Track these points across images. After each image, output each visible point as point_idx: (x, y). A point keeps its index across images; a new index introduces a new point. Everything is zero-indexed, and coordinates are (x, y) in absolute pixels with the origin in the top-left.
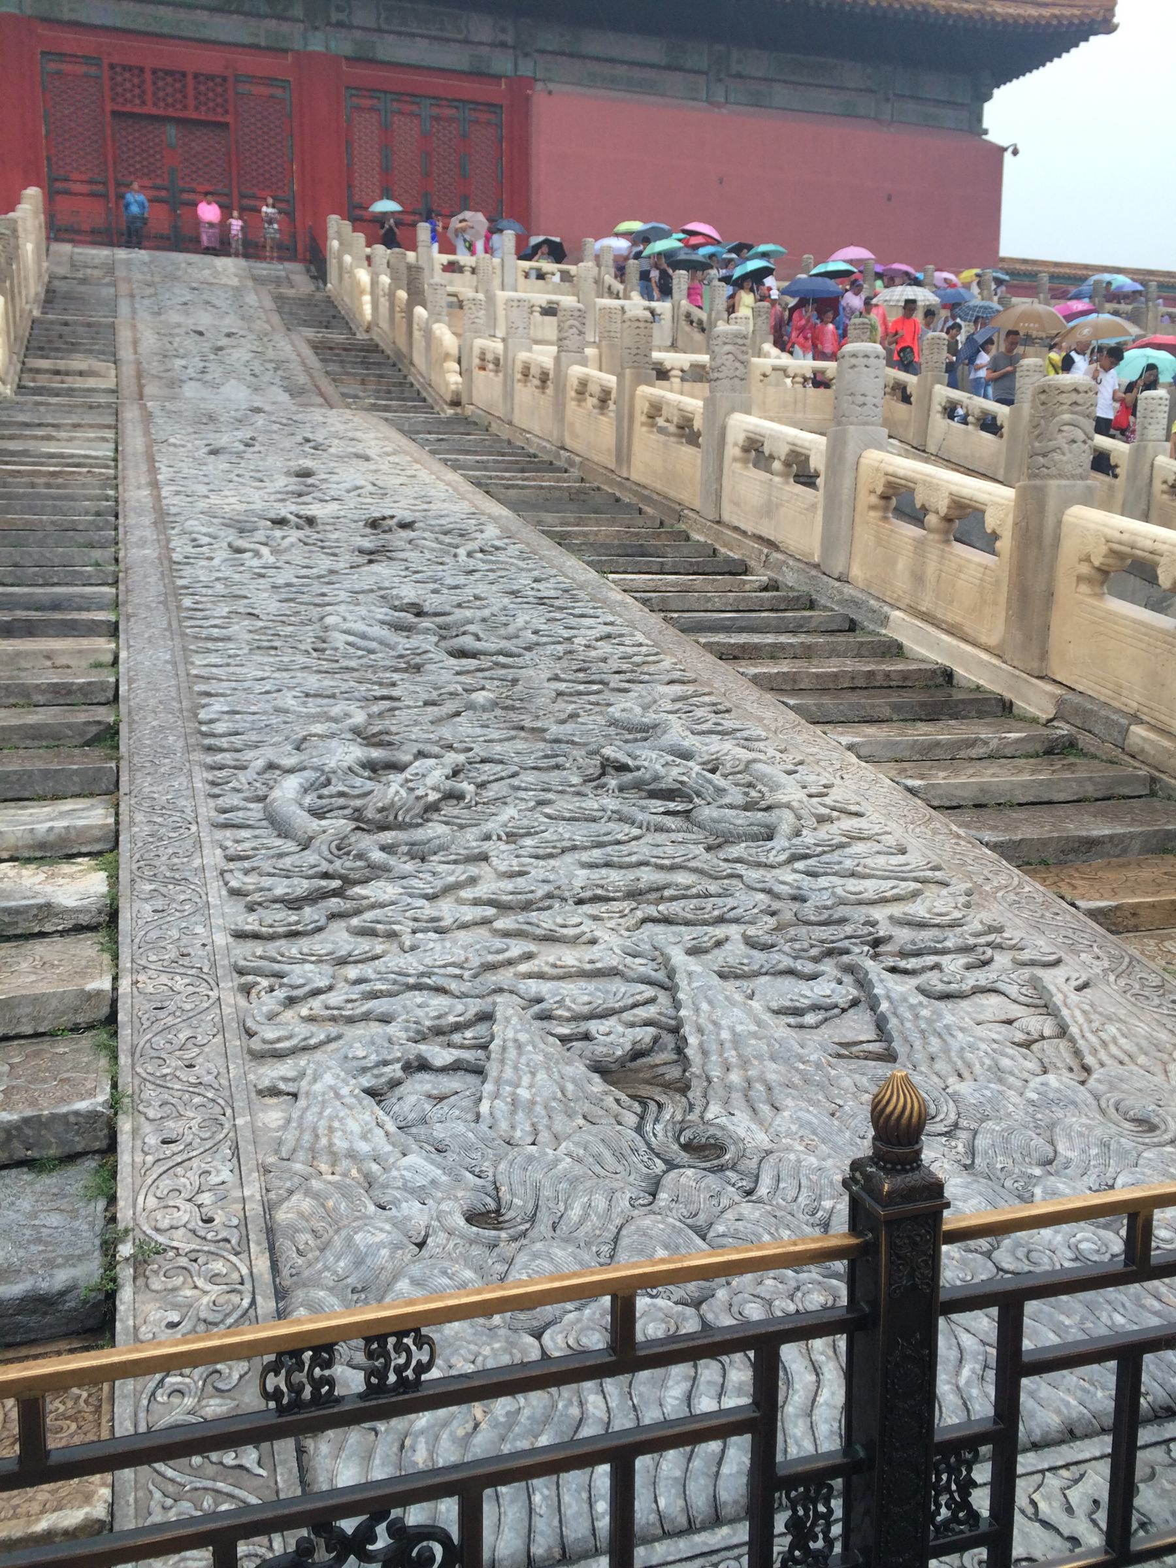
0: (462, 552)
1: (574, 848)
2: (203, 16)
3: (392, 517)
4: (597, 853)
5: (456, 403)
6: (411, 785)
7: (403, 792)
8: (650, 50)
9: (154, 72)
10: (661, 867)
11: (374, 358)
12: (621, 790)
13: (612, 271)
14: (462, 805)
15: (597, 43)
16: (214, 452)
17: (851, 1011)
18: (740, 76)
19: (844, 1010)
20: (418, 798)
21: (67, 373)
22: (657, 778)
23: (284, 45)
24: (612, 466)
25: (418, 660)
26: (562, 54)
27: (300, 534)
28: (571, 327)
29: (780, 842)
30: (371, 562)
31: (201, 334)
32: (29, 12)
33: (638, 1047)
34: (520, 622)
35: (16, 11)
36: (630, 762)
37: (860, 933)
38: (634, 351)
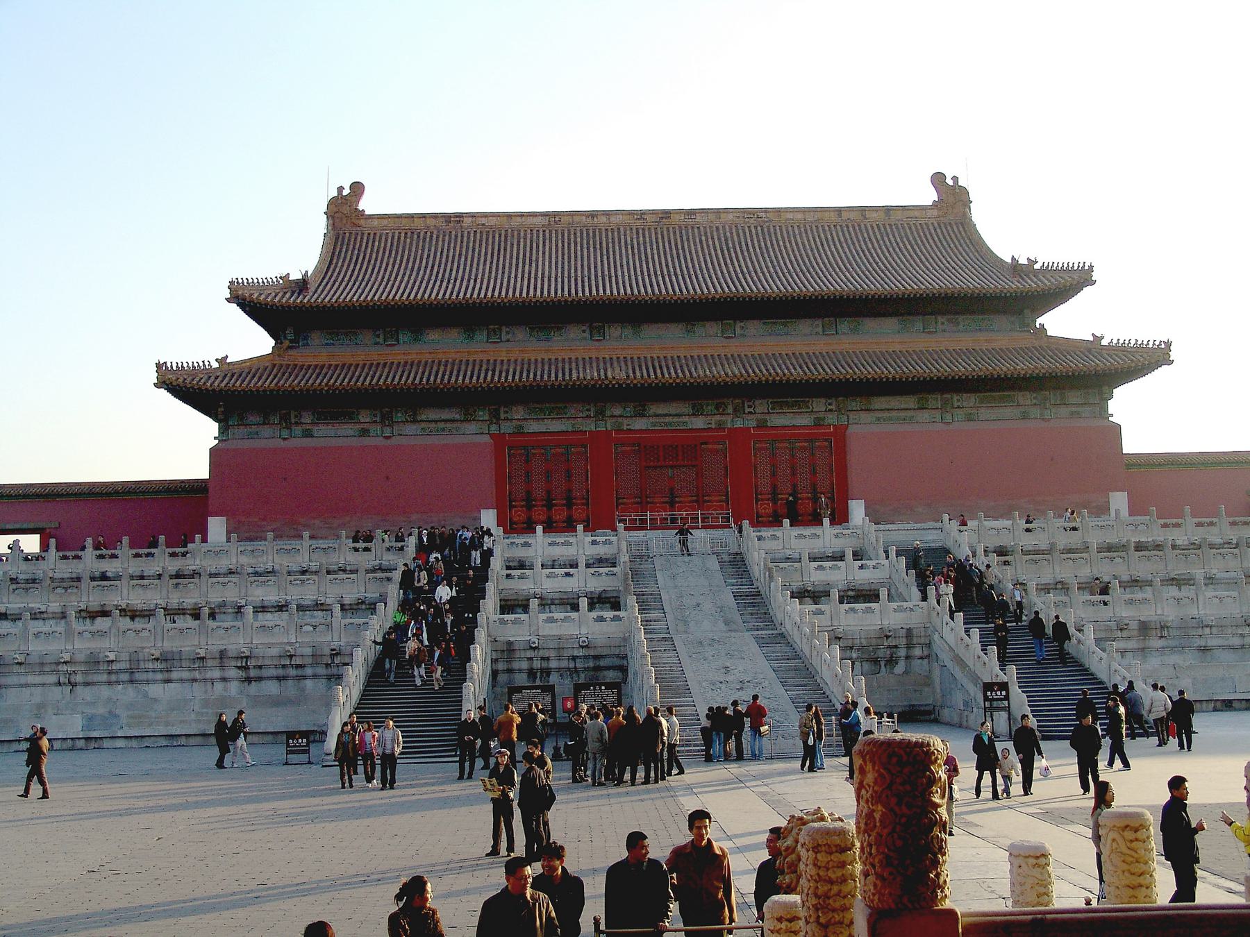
2: (686, 419)
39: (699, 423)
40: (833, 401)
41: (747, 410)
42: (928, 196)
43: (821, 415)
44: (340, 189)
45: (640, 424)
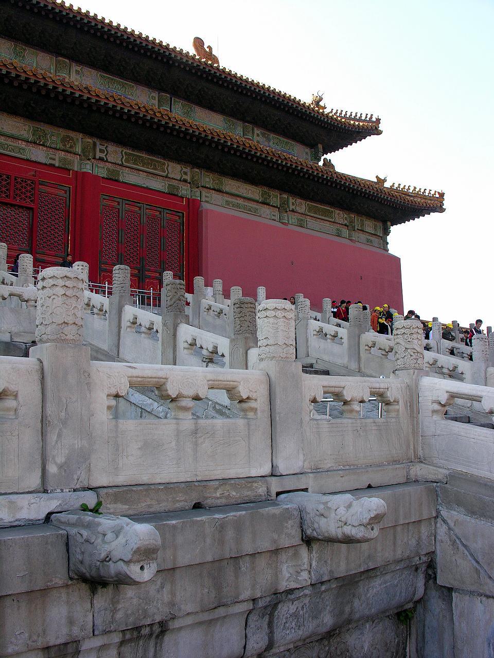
2: (23, 145)
15: (231, 185)
18: (293, 211)
23: (70, 167)
26: (214, 189)
40: (188, 170)
41: (98, 155)
43: (175, 183)
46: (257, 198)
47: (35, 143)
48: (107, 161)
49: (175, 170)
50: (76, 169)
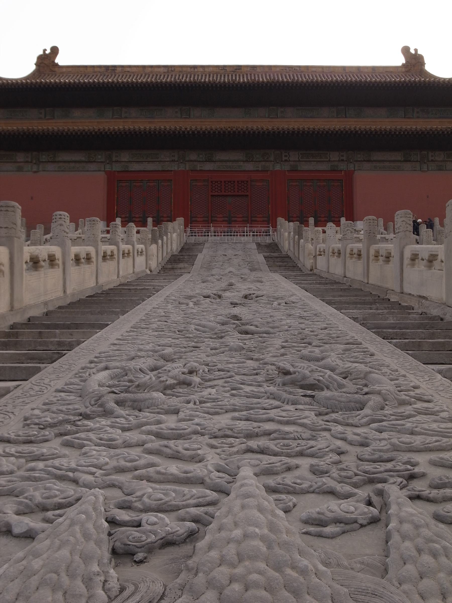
0: (275, 303)
1: (234, 410)
2: (241, 163)
3: (254, 294)
4: (244, 413)
5: (311, 270)
6: (160, 375)
7: (154, 378)
8: (398, 156)
9: (225, 182)
10: (280, 422)
11: (286, 259)
12: (284, 384)
13: (383, 228)
14: (189, 388)
15: (377, 156)
16: (203, 282)
17: (369, 527)
18: (432, 161)
19: (362, 526)
20: (161, 382)
21: (176, 269)
22: (304, 378)
24: (362, 280)
25: (223, 335)
26: (364, 161)
27: (213, 300)
28: (347, 230)
29: (367, 411)
30: (234, 307)
31: (226, 255)
32: (187, 169)
33: (170, 537)
34: (284, 322)
35: (184, 169)
36: (292, 369)
37: (398, 468)
38: (368, 232)
39: (250, 167)
41: (284, 158)
42: (399, 60)
44: (45, 50)
45: (208, 166)
46: (399, 158)
47: (247, 161)
48: (290, 161)
49: (334, 156)
50: (271, 169)
